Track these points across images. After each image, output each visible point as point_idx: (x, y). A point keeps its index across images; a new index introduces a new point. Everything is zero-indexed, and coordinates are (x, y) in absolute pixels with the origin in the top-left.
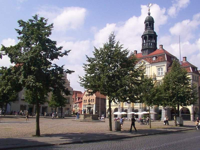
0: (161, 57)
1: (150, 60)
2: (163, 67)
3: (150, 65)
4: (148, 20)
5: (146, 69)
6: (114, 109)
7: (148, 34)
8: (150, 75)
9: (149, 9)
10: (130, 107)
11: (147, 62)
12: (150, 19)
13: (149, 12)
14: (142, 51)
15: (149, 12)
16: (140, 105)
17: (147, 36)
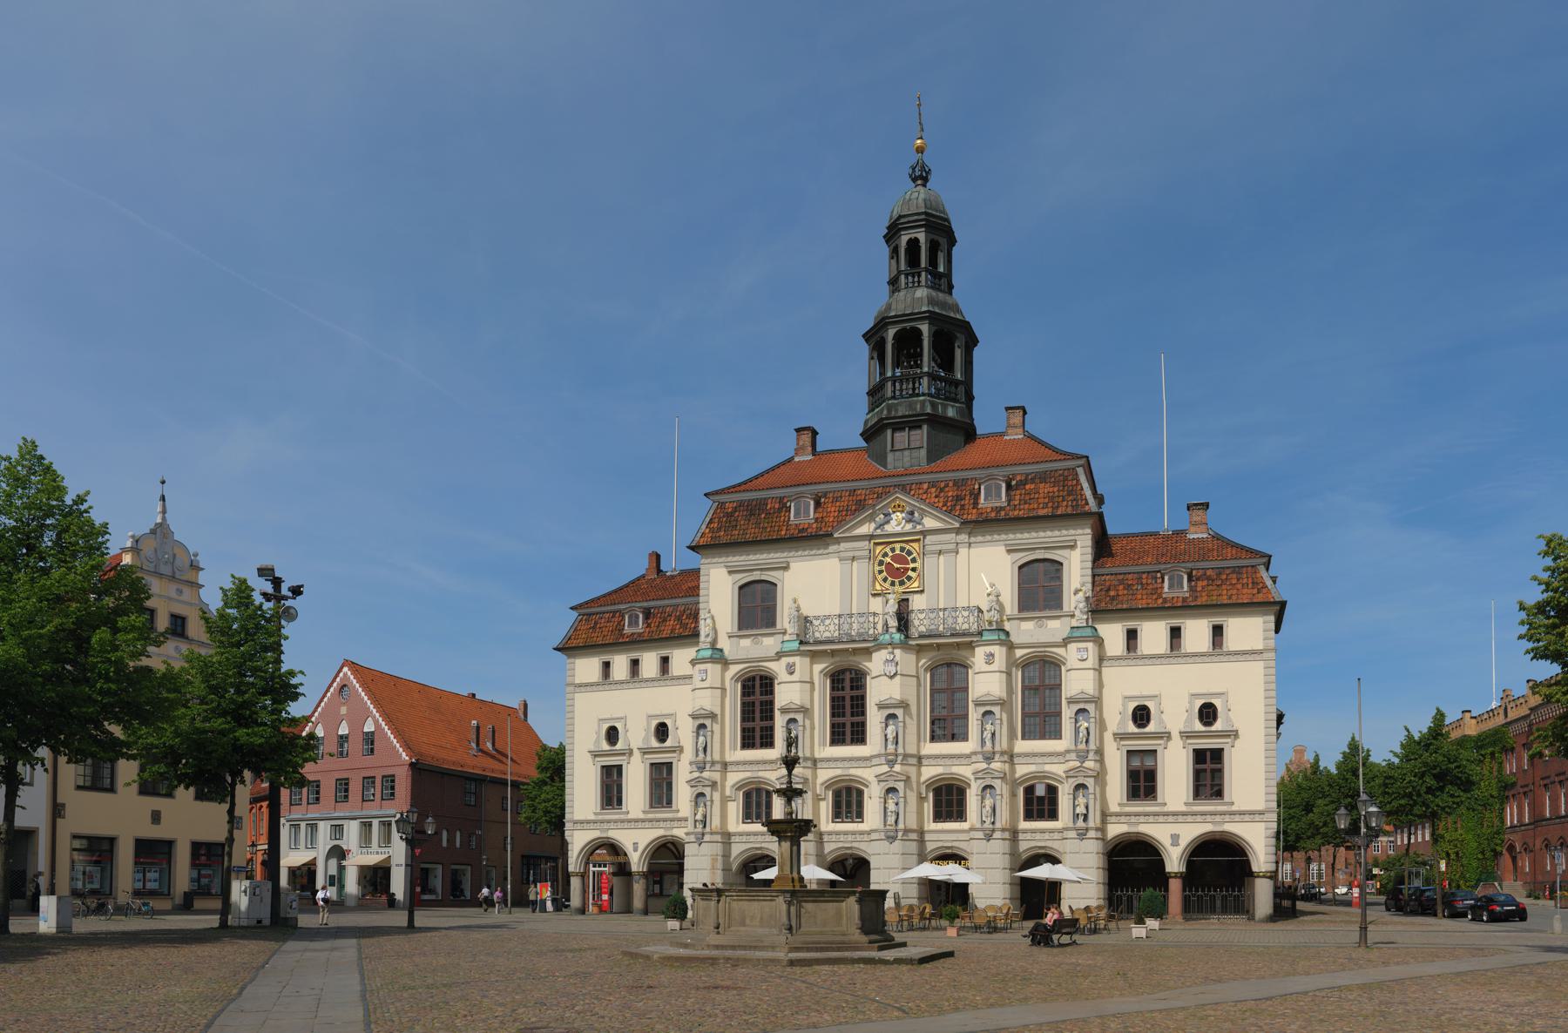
0: (1045, 489)
1: (958, 498)
3: (958, 531)
4: (926, 213)
5: (930, 561)
6: (641, 848)
7: (932, 317)
11: (932, 505)
12: (931, 209)
16: (891, 820)
17: (925, 328)
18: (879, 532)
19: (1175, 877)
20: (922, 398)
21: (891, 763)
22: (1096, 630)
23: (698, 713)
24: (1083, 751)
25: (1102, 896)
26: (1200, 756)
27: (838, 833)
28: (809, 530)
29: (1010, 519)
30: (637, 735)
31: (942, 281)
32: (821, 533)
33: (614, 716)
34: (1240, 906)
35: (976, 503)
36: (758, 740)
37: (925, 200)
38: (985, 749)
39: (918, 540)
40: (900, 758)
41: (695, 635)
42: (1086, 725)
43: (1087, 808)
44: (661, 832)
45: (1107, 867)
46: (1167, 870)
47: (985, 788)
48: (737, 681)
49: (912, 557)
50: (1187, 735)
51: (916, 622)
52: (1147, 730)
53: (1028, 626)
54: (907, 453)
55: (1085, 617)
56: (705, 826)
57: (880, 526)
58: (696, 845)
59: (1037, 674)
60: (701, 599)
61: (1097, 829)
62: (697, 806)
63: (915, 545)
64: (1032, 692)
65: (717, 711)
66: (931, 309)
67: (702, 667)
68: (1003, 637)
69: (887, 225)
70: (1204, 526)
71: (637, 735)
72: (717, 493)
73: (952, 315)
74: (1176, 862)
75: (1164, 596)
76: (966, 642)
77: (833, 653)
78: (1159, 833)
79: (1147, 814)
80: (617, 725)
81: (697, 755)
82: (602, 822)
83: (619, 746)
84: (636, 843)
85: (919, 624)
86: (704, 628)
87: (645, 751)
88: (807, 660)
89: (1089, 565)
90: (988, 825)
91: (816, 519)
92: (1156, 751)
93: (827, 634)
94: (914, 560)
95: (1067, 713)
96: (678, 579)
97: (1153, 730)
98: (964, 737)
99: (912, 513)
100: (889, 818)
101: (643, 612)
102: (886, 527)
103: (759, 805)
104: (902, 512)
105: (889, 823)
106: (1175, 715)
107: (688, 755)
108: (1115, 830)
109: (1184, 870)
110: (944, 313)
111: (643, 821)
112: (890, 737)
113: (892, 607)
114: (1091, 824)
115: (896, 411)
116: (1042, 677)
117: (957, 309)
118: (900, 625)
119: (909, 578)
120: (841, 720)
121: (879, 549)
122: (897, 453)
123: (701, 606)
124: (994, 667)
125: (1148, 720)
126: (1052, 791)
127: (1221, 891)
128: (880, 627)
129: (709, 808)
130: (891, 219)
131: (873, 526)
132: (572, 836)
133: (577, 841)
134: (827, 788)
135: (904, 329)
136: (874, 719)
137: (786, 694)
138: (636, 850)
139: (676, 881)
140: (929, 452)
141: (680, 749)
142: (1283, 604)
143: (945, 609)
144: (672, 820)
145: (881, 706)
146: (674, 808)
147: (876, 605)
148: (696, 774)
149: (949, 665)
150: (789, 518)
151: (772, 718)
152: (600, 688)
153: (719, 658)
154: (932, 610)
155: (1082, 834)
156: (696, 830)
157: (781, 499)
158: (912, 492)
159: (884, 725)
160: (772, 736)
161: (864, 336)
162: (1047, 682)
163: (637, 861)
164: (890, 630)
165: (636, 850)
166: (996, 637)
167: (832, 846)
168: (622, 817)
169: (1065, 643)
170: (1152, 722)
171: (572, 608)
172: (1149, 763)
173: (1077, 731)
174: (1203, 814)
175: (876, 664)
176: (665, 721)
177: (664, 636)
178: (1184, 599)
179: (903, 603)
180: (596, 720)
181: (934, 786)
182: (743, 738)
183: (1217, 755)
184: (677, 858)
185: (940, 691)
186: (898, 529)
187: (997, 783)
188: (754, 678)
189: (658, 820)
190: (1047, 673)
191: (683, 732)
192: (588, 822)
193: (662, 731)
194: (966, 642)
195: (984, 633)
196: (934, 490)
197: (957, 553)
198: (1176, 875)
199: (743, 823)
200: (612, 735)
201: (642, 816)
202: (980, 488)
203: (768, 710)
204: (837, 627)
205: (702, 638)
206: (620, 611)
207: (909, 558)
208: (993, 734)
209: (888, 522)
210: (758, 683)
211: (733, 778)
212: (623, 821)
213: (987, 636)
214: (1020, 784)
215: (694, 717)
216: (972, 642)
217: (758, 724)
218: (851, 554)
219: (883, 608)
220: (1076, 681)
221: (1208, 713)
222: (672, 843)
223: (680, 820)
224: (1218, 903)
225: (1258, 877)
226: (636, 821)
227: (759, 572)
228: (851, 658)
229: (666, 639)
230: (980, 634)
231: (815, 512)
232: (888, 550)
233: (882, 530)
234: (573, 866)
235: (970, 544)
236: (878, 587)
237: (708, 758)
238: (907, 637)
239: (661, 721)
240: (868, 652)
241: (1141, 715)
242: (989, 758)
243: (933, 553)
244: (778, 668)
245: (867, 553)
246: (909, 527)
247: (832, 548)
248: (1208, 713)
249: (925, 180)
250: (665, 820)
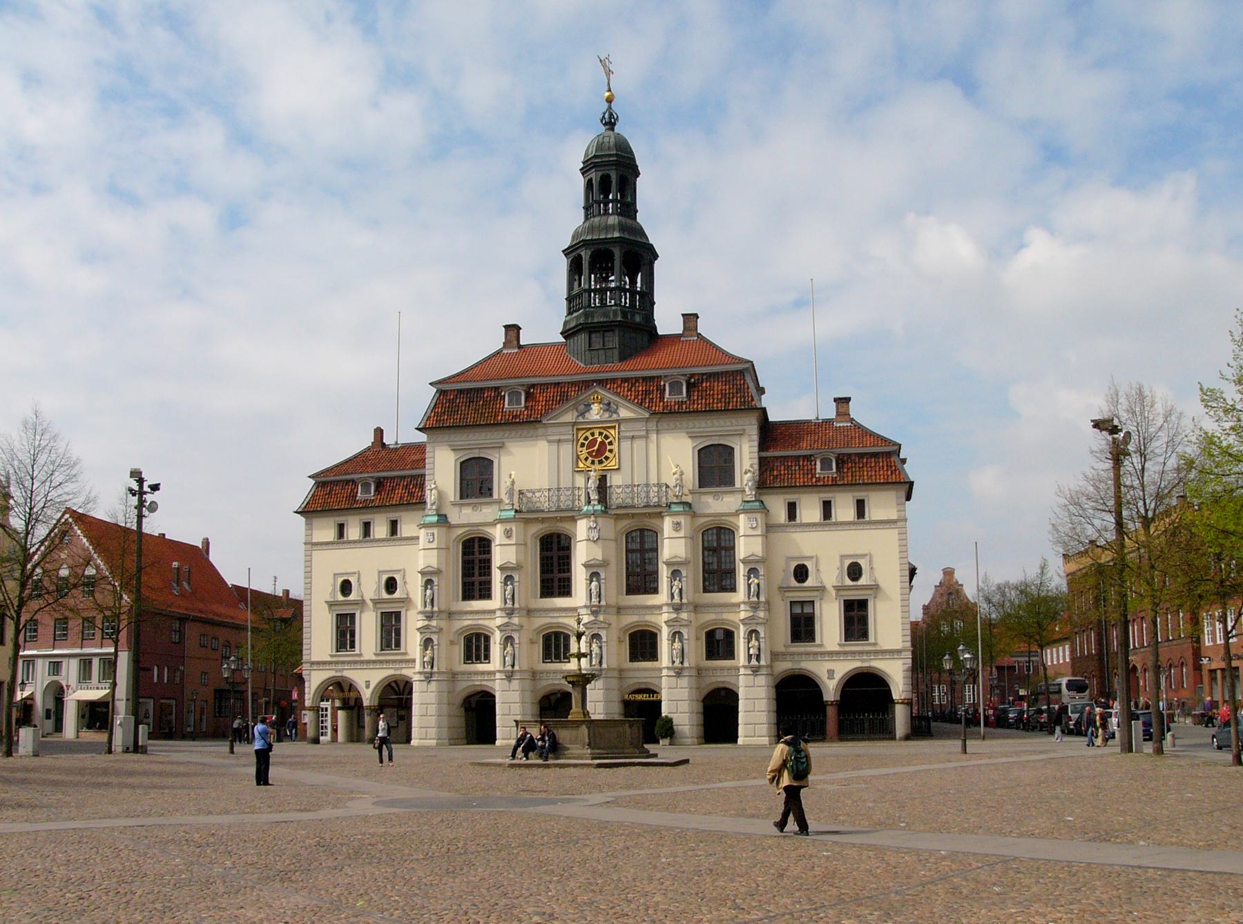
0: (718, 386)
1: (647, 393)
2: (736, 439)
3: (647, 420)
4: (616, 155)
6: (372, 686)
8: (653, 480)
9: (607, 94)
10: (516, 668)
11: (625, 398)
13: (610, 108)
14: (568, 333)
15: (610, 108)
17: (617, 253)
18: (581, 419)
19: (832, 704)
20: (613, 308)
21: (595, 613)
22: (762, 502)
23: (426, 570)
24: (753, 602)
25: (773, 722)
27: (548, 672)
28: (521, 417)
29: (690, 412)
30: (369, 588)
31: (628, 208)
32: (532, 419)
33: (349, 571)
34: (884, 731)
35: (662, 398)
36: (477, 593)
37: (616, 145)
38: (674, 601)
39: (614, 427)
40: (603, 609)
41: (422, 502)
42: (756, 581)
43: (759, 649)
44: (391, 672)
45: (775, 697)
46: (825, 699)
47: (675, 633)
48: (458, 542)
49: (609, 440)
50: (838, 589)
51: (614, 496)
52: (806, 584)
53: (709, 499)
54: (601, 352)
55: (754, 493)
56: (432, 667)
57: (582, 414)
58: (425, 683)
59: (715, 537)
60: (427, 472)
61: (767, 666)
62: (426, 648)
63: (612, 432)
64: (711, 553)
65: (443, 568)
66: (622, 235)
67: (430, 531)
68: (687, 509)
69: (582, 160)
70: (846, 417)
71: (369, 588)
72: (439, 382)
73: (639, 240)
74: (832, 692)
75: (817, 476)
76: (658, 511)
77: (543, 520)
79: (808, 654)
80: (350, 579)
81: (425, 606)
82: (337, 663)
83: (352, 597)
84: (368, 683)
86: (430, 497)
87: (376, 602)
88: (522, 525)
89: (756, 449)
90: (677, 664)
91: (526, 407)
92: (813, 602)
93: (538, 505)
94: (610, 443)
95: (741, 571)
96: (401, 452)
97: (811, 585)
98: (655, 591)
99: (609, 404)
100: (594, 660)
101: (374, 482)
102: (587, 415)
103: (478, 648)
104: (600, 403)
105: (594, 663)
106: (828, 574)
107: (419, 605)
109: (839, 698)
110: (632, 238)
111: (374, 662)
113: (593, 484)
114: (763, 663)
115: (593, 318)
116: (719, 539)
117: (641, 232)
118: (600, 497)
119: (607, 458)
120: (550, 576)
121: (581, 433)
122: (593, 352)
123: (427, 478)
124: (682, 534)
125: (807, 577)
126: (729, 635)
127: (869, 716)
128: (583, 498)
129: (436, 652)
130: (586, 155)
131: (576, 414)
132: (310, 675)
133: (314, 680)
134: (625, 632)
135: (600, 250)
136: (579, 576)
137: (501, 555)
138: (368, 687)
139: (396, 714)
140: (620, 352)
141: (406, 601)
142: (911, 484)
143: (638, 485)
144: (401, 661)
146: (403, 650)
147: (580, 481)
148: (426, 623)
149: (642, 531)
150: (504, 405)
151: (489, 574)
152: (335, 546)
153: (443, 519)
154: (627, 486)
155: (756, 671)
156: (425, 670)
157: (496, 389)
158: (608, 386)
159: (588, 582)
160: (489, 589)
161: (563, 251)
162: (723, 544)
163: (368, 696)
164: (592, 503)
165: (368, 687)
166: (682, 509)
167: (544, 683)
168: (357, 659)
169: (737, 514)
170: (810, 578)
171: (309, 477)
172: (807, 610)
173: (749, 586)
174: (853, 653)
175: (582, 529)
176: (395, 576)
177: (394, 503)
178: (834, 479)
179: (603, 480)
180: (332, 576)
181: (630, 632)
182: (464, 591)
183: (863, 604)
184: (397, 695)
185: (633, 551)
186: (597, 417)
187: (684, 631)
188: (472, 540)
189: (388, 662)
190: (723, 537)
191: (413, 587)
192: (324, 663)
193: (391, 585)
194: (658, 511)
195: (673, 506)
196: (626, 385)
197: (647, 437)
199: (465, 663)
200: (346, 587)
201: (374, 658)
202: (664, 385)
204: (547, 499)
205: (429, 506)
206: (353, 481)
207: (607, 442)
208: (681, 590)
209: (589, 411)
210: (476, 541)
212: (355, 662)
213: (675, 508)
214: (703, 629)
215: (423, 573)
216: (661, 512)
217: (477, 578)
218: (557, 438)
219: (586, 484)
220: (746, 546)
222: (395, 682)
223: (408, 661)
224: (866, 725)
225: (898, 703)
226: (368, 662)
227: (478, 450)
228: (558, 524)
229: (396, 505)
230: (669, 506)
231: (526, 401)
232: (588, 434)
233: (583, 418)
234: (311, 701)
235: (658, 431)
236: (581, 465)
237: (436, 609)
238: (606, 507)
239: (391, 576)
240: (573, 520)
241: (801, 573)
242: (678, 608)
243: (626, 438)
244: (497, 534)
245: (570, 437)
246: (607, 415)
247: (541, 431)
248: (855, 571)
249: (614, 124)
250: (394, 661)
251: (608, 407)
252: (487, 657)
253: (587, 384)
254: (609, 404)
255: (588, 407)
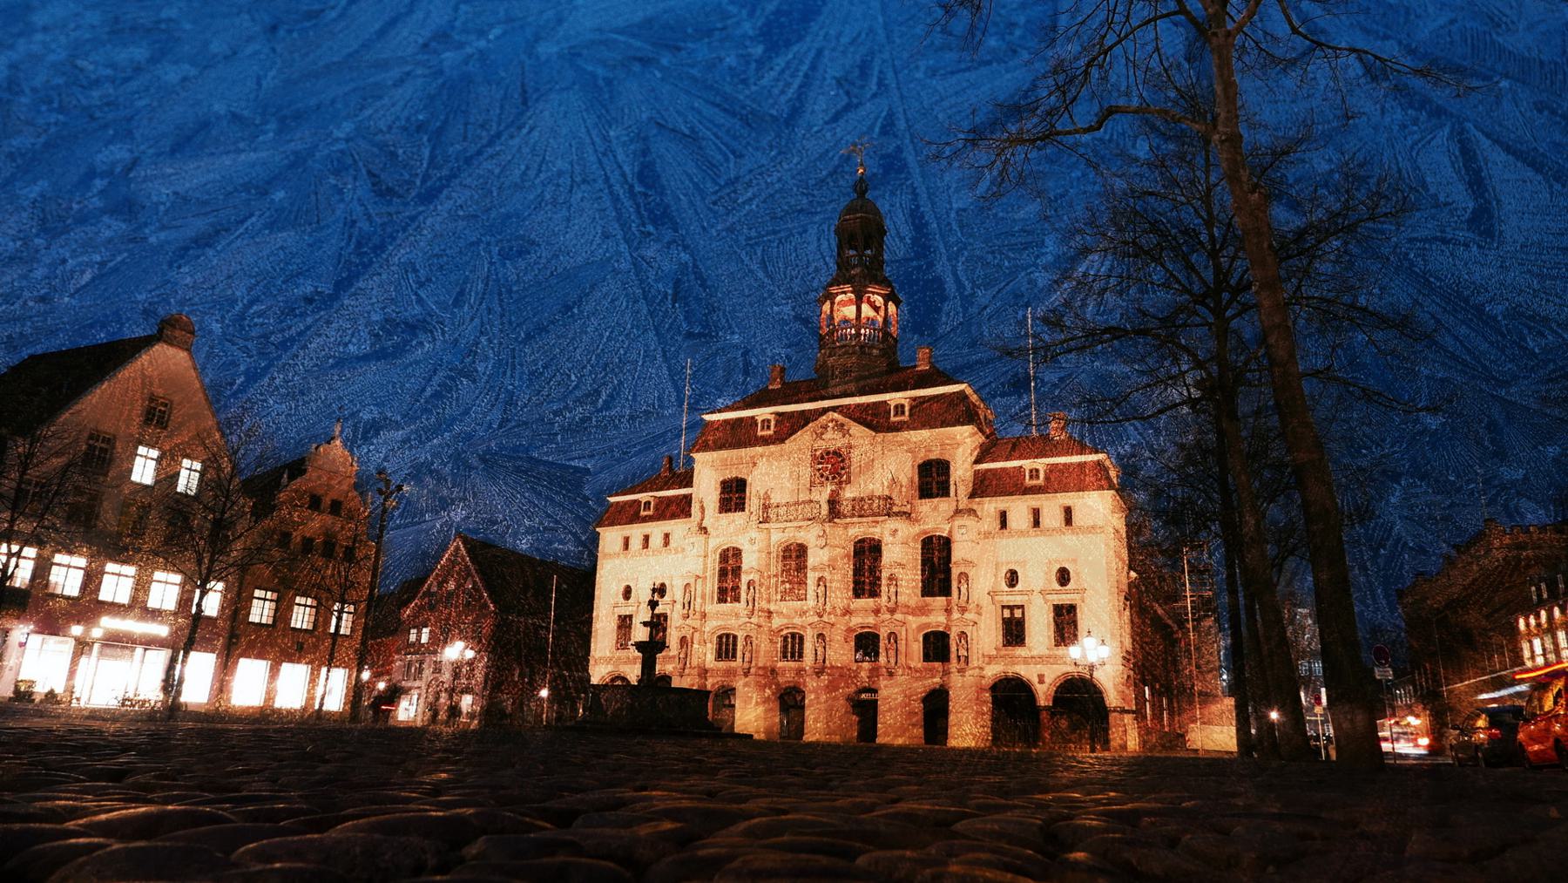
16: (820, 658)
21: (820, 616)
26: (1058, 610)
78: (1028, 672)
85: (846, 507)
106: (1037, 578)
107: (679, 606)
108: (993, 671)
112: (820, 595)
137: (750, 561)
145: (814, 569)
172: (1018, 613)
183: (1072, 609)
198: (1046, 708)
203: (737, 571)
211: (711, 625)
221: (1064, 577)
248: (1064, 577)
251: (840, 427)
252: (734, 656)
253: (825, 411)
254: (842, 425)
255: (825, 427)
